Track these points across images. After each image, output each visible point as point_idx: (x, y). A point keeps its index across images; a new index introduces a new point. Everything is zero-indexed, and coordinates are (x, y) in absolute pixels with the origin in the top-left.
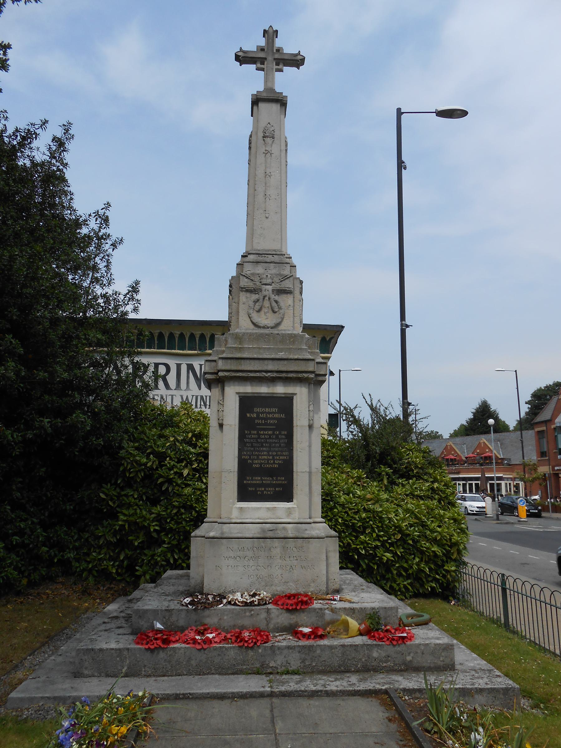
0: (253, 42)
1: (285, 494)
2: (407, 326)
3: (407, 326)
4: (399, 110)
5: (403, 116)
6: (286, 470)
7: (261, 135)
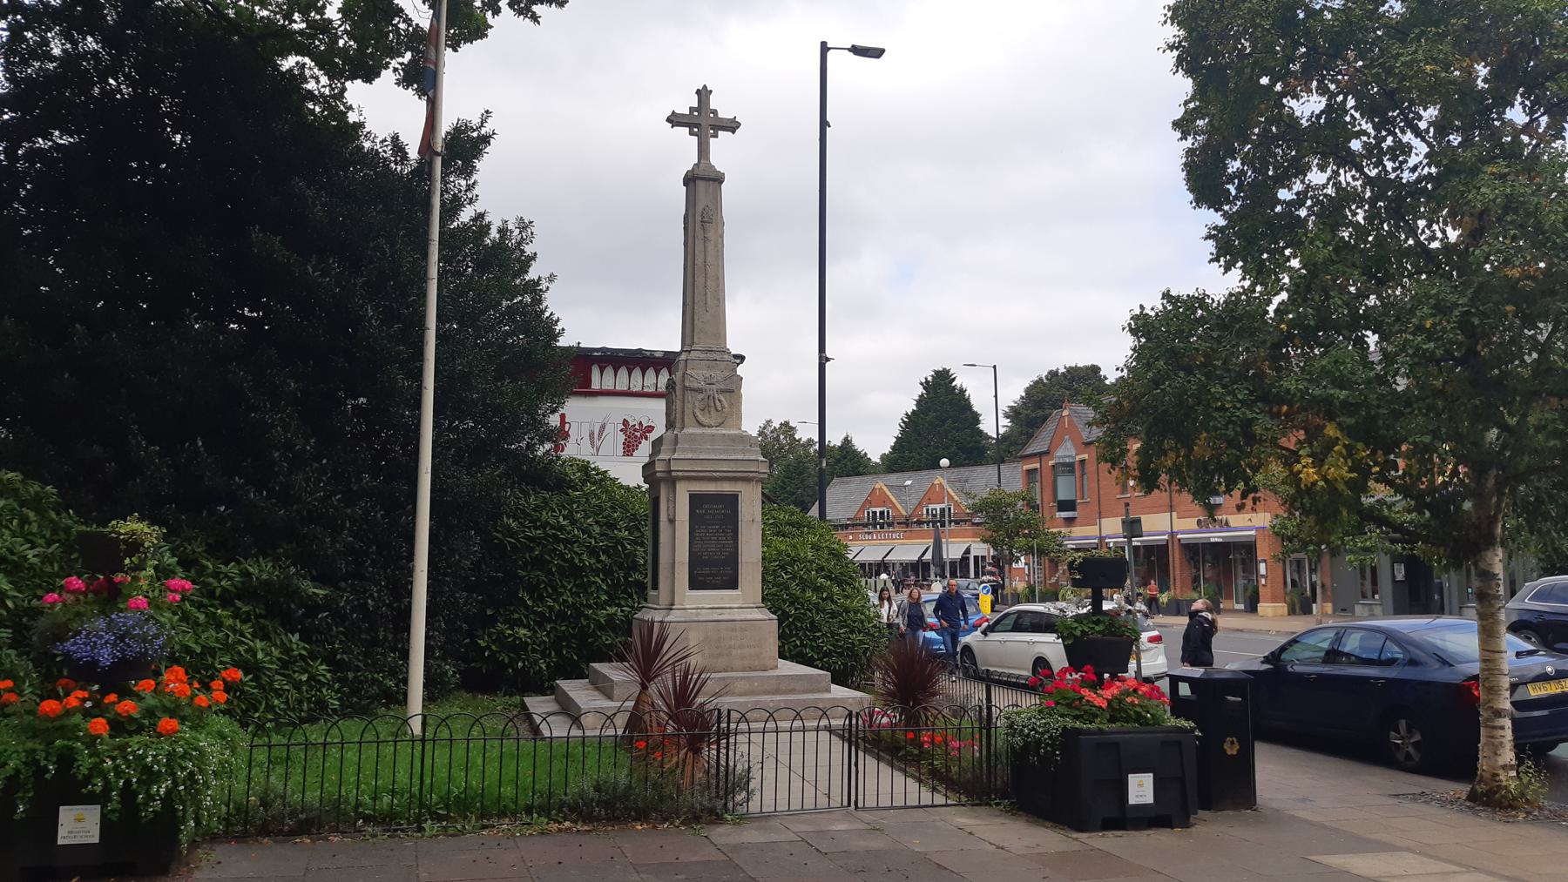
0: (686, 103)
1: (732, 584)
2: (828, 360)
3: (828, 360)
4: (824, 44)
5: (830, 54)
6: (733, 560)
7: (699, 218)
